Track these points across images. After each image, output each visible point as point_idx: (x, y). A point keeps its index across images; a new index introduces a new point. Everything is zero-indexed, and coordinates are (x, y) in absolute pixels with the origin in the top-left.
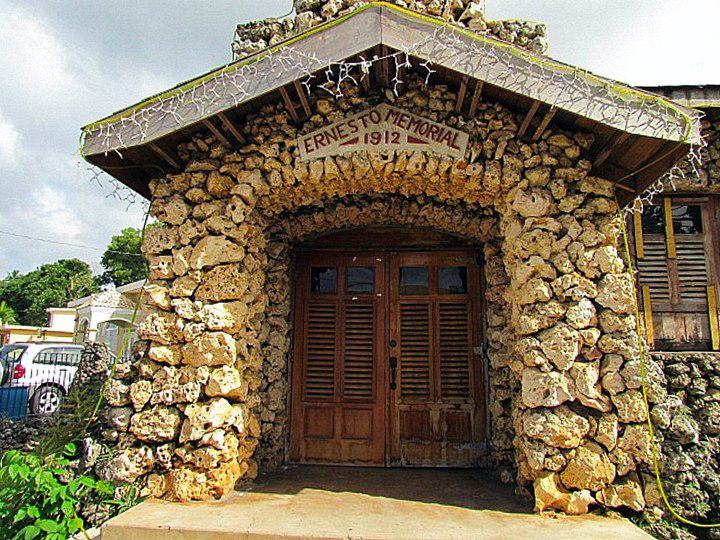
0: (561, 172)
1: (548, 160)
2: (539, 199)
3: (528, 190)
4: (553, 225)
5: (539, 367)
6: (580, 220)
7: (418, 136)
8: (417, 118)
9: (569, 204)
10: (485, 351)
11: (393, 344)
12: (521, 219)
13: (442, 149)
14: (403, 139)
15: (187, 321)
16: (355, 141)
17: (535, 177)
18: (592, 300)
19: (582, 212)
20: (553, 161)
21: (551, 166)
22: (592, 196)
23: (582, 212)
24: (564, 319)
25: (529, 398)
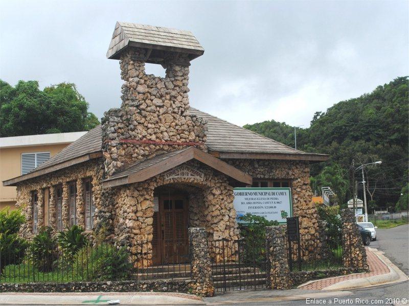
0: (223, 184)
1: (221, 181)
3: (216, 188)
5: (217, 231)
7: (192, 174)
9: (224, 192)
11: (163, 226)
12: (214, 195)
13: (198, 177)
14: (189, 175)
16: (178, 175)
17: (218, 185)
22: (229, 190)
24: (222, 220)
25: (215, 238)
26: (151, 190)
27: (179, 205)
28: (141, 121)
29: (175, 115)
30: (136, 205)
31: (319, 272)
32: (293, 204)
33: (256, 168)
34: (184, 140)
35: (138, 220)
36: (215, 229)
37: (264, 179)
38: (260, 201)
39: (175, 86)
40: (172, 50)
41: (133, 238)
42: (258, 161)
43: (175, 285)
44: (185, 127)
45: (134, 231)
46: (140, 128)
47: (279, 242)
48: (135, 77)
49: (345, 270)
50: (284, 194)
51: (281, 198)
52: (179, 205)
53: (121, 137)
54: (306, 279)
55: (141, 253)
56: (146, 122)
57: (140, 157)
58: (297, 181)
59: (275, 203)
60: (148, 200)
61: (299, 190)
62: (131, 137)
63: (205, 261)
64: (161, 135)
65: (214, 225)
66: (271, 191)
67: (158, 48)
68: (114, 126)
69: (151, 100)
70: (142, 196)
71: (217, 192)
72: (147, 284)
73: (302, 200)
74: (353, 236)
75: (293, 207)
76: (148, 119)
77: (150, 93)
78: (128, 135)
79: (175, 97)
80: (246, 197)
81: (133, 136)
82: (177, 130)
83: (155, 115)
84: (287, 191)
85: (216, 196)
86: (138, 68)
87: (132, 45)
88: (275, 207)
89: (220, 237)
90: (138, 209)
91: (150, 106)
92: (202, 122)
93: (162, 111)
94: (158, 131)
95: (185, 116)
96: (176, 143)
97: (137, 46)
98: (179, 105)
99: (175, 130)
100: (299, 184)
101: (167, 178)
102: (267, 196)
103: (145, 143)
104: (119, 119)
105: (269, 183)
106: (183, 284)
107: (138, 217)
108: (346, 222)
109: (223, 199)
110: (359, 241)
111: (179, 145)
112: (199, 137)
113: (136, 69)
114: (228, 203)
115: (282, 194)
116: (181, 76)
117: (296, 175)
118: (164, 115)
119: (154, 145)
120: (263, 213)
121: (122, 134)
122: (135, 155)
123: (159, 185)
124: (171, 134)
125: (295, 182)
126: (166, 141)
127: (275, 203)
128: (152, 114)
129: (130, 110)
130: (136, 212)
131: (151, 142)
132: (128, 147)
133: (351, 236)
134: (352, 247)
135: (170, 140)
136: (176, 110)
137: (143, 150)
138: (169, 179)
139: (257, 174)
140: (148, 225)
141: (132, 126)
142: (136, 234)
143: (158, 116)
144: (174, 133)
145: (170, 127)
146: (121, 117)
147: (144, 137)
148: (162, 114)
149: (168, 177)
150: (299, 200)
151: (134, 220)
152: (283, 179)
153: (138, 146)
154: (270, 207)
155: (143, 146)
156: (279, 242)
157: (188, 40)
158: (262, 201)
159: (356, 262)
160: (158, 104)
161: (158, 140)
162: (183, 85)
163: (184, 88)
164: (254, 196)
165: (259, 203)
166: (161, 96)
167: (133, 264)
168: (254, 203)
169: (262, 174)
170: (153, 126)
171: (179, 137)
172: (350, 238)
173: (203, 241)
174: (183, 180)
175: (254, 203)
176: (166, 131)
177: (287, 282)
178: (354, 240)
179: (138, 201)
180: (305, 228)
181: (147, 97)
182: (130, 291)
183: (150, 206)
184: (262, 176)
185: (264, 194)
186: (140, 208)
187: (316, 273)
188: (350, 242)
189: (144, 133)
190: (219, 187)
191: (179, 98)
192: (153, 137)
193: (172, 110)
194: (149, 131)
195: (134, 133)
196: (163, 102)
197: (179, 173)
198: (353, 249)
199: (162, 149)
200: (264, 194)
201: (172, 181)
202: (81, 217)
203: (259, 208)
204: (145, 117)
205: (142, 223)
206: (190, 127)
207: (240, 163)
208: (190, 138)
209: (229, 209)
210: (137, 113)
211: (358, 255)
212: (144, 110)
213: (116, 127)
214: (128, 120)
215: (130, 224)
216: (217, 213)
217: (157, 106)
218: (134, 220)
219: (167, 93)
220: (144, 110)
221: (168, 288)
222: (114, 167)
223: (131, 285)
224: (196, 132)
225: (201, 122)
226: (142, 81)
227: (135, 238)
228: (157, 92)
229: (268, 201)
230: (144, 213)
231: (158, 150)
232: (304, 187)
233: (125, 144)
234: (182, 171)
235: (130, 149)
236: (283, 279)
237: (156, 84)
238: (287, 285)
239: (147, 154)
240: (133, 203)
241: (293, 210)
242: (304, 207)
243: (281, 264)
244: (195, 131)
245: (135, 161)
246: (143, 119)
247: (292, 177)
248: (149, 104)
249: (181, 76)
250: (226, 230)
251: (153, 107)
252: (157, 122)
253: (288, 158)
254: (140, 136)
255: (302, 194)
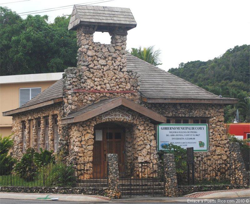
0: (146, 122)
1: (144, 120)
2: (142, 127)
3: (140, 125)
4: (144, 132)
5: (141, 156)
6: (148, 131)
8: (123, 112)
9: (147, 128)
10: (125, 152)
11: (105, 151)
12: (139, 130)
13: (127, 118)
14: (120, 116)
15: (85, 149)
16: (112, 116)
17: (142, 123)
18: (150, 144)
19: (149, 129)
20: (145, 120)
21: (144, 121)
23: (149, 129)
24: (145, 148)
26: (92, 126)
27: (118, 136)
28: (90, 77)
29: (115, 71)
30: (80, 137)
31: (205, 187)
32: (209, 136)
33: (179, 109)
34: (122, 89)
35: (82, 147)
36: (140, 154)
37: (185, 117)
38: (182, 134)
39: (116, 50)
40: (112, 25)
41: (78, 159)
42: (180, 104)
43: (97, 191)
44: (123, 80)
45: (79, 155)
46: (89, 81)
47: (171, 165)
48: (86, 45)
49: (228, 186)
50: (202, 128)
51: (199, 132)
52: (118, 136)
53: (75, 88)
54: (193, 191)
55: (84, 170)
56: (94, 77)
57: (89, 102)
58: (213, 119)
59: (194, 135)
60: (90, 133)
61: (214, 125)
62: (82, 88)
63: (115, 175)
64: (105, 86)
65: (139, 151)
66: (191, 126)
67: (102, 24)
68: (70, 80)
69: (97, 60)
70: (86, 130)
71: (141, 128)
72: (80, 189)
73: (216, 133)
74: (238, 162)
75: (209, 139)
76: (95, 74)
77: (97, 56)
78: (80, 87)
79: (116, 58)
80: (171, 131)
81: (83, 88)
82: (117, 82)
83: (101, 71)
84: (205, 127)
85: (140, 131)
86: (88, 38)
87: (82, 23)
88: (194, 139)
89: (142, 160)
90: (82, 140)
91: (97, 65)
92: (136, 76)
93: (105, 68)
94: (103, 83)
95: (123, 72)
96: (115, 92)
97: (86, 24)
98: (119, 64)
99: (115, 82)
100: (215, 121)
101: (103, 118)
102: (188, 130)
103: (92, 91)
104: (74, 75)
105: (190, 121)
106: (102, 190)
107: (82, 145)
108: (233, 152)
109: (146, 133)
110: (241, 166)
111: (117, 93)
112: (133, 87)
113: (87, 39)
114: (149, 136)
115: (200, 128)
116: (120, 43)
117: (212, 114)
118: (107, 72)
119: (99, 93)
120: (184, 143)
121: (76, 86)
122: (85, 101)
123: (98, 123)
124: (112, 85)
125: (211, 120)
126: (108, 90)
127: (194, 135)
128: (98, 71)
129: (82, 69)
130: (81, 141)
131: (97, 91)
132: (80, 95)
133: (236, 162)
134: (236, 170)
135: (112, 90)
136: (116, 68)
137: (91, 97)
138: (105, 119)
139: (179, 114)
140: (89, 150)
141: (83, 80)
142: (81, 157)
143: (103, 72)
144: (114, 85)
145: (111, 80)
146: (75, 73)
147: (92, 87)
148: (106, 71)
149: (104, 117)
150: (214, 134)
151: (79, 147)
152: (201, 117)
153: (87, 94)
154: (190, 139)
155: (91, 94)
156: (171, 165)
157: (126, 17)
158: (183, 134)
159: (238, 181)
160: (103, 64)
161: (102, 90)
162: (122, 49)
163: (122, 51)
164: (176, 130)
165: (181, 135)
166: (105, 58)
167: (78, 177)
168: (177, 135)
169: (184, 114)
170: (99, 80)
171: (118, 87)
172: (235, 163)
173: (115, 162)
174: (116, 119)
175: (177, 135)
176: (108, 83)
177: (175, 192)
178: (238, 165)
179: (82, 134)
180: (218, 155)
181: (95, 59)
182: (69, 193)
183: (90, 138)
184: (183, 115)
185: (185, 128)
186: (83, 139)
187: (201, 187)
188: (235, 167)
189: (92, 85)
190: (143, 124)
191: (119, 59)
192: (99, 88)
193: (113, 67)
194: (96, 83)
195: (84, 84)
196: (107, 62)
197: (113, 114)
198: (237, 171)
199: (105, 96)
200: (185, 128)
201: (108, 120)
202: (51, 142)
203: (181, 139)
204: (93, 73)
205: (85, 149)
206: (127, 80)
207: (165, 105)
208: (127, 88)
209: (150, 140)
210: (87, 70)
211: (240, 176)
212: (92, 68)
213: (71, 81)
214: (80, 76)
215: (76, 149)
216: (141, 143)
217: (101, 65)
218: (79, 147)
219: (109, 56)
220: (92, 68)
221: (92, 192)
222: (70, 109)
223: (70, 190)
224: (131, 83)
225: (135, 76)
226: (91, 48)
227: (80, 159)
228: (102, 55)
229: (188, 134)
230: (87, 142)
231: (102, 97)
232: (219, 123)
233: (78, 93)
234: (115, 113)
235: (81, 97)
236: (172, 190)
237: (101, 49)
238: (174, 194)
239: (93, 100)
240: (79, 135)
241: (209, 141)
242: (218, 139)
243: (171, 180)
244: (131, 82)
245: (85, 105)
246: (92, 75)
247: (209, 116)
248: (96, 64)
249: (120, 43)
250: (147, 156)
251: (99, 66)
252: (102, 77)
253: (203, 102)
254: (89, 87)
255: (216, 129)
